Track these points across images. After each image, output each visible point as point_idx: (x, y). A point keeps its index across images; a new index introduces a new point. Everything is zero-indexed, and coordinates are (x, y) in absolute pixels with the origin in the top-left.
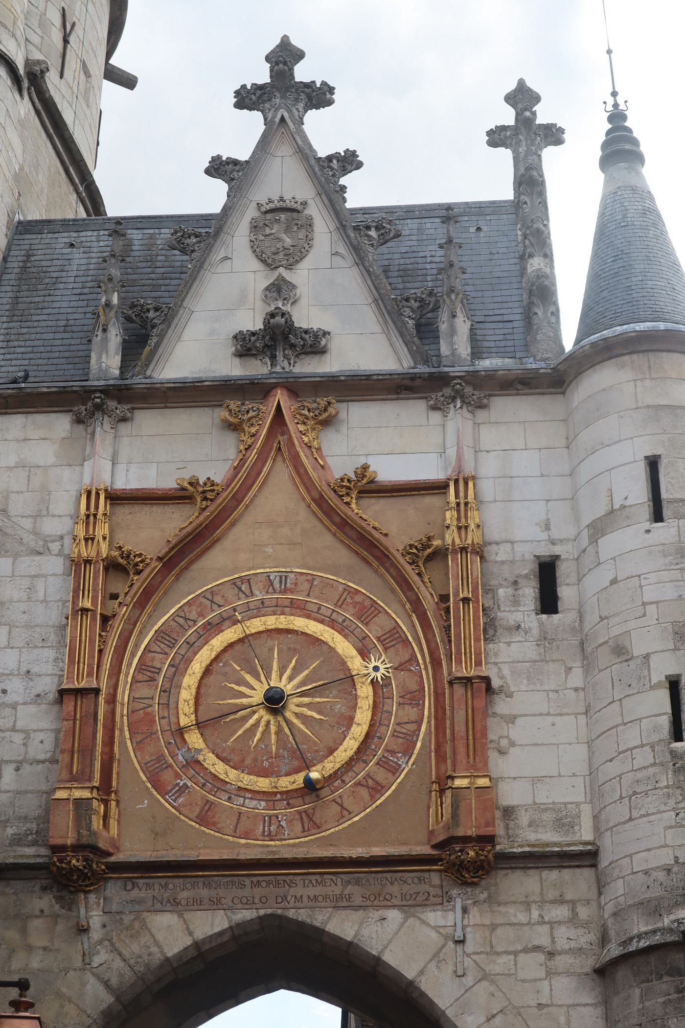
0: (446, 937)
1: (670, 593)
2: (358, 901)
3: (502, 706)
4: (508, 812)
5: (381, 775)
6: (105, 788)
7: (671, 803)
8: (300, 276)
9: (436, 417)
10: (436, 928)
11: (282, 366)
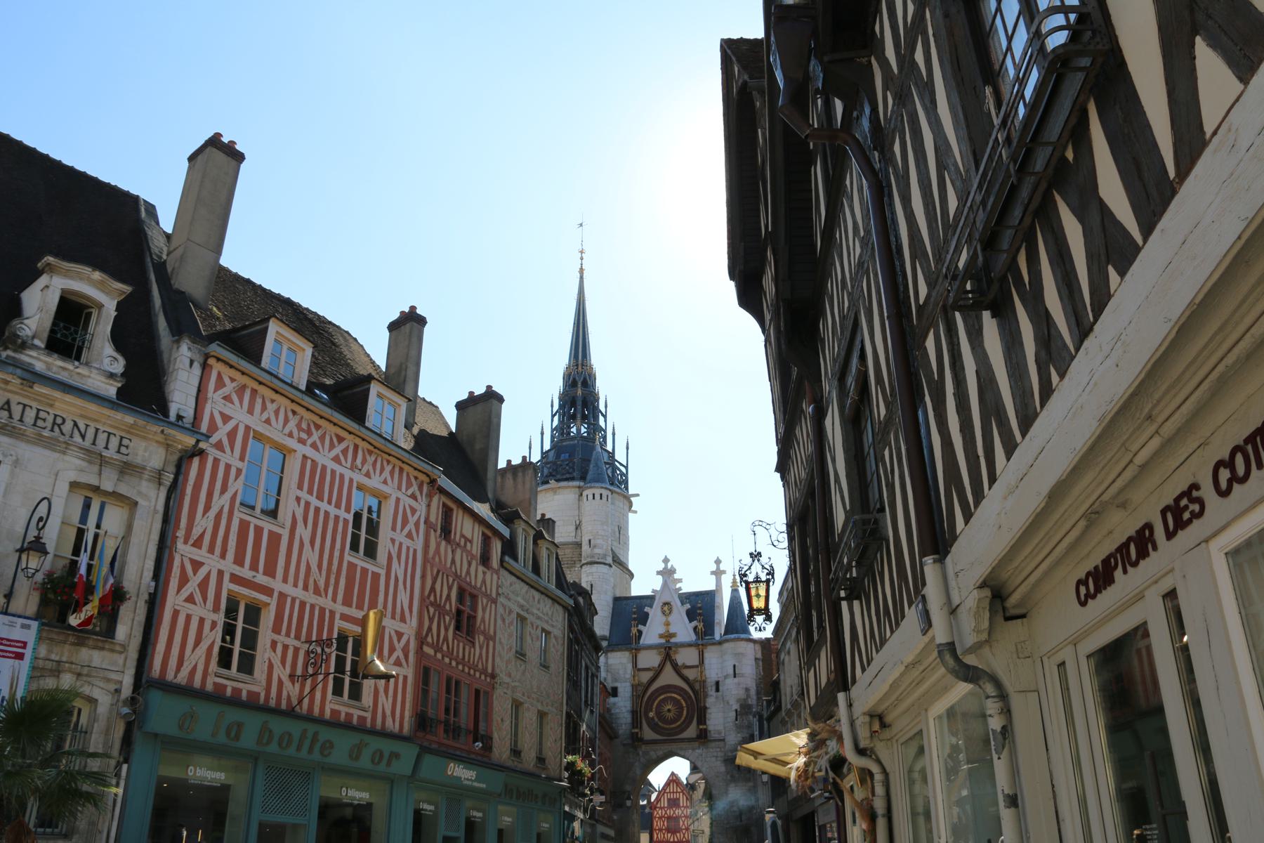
8: (670, 619)
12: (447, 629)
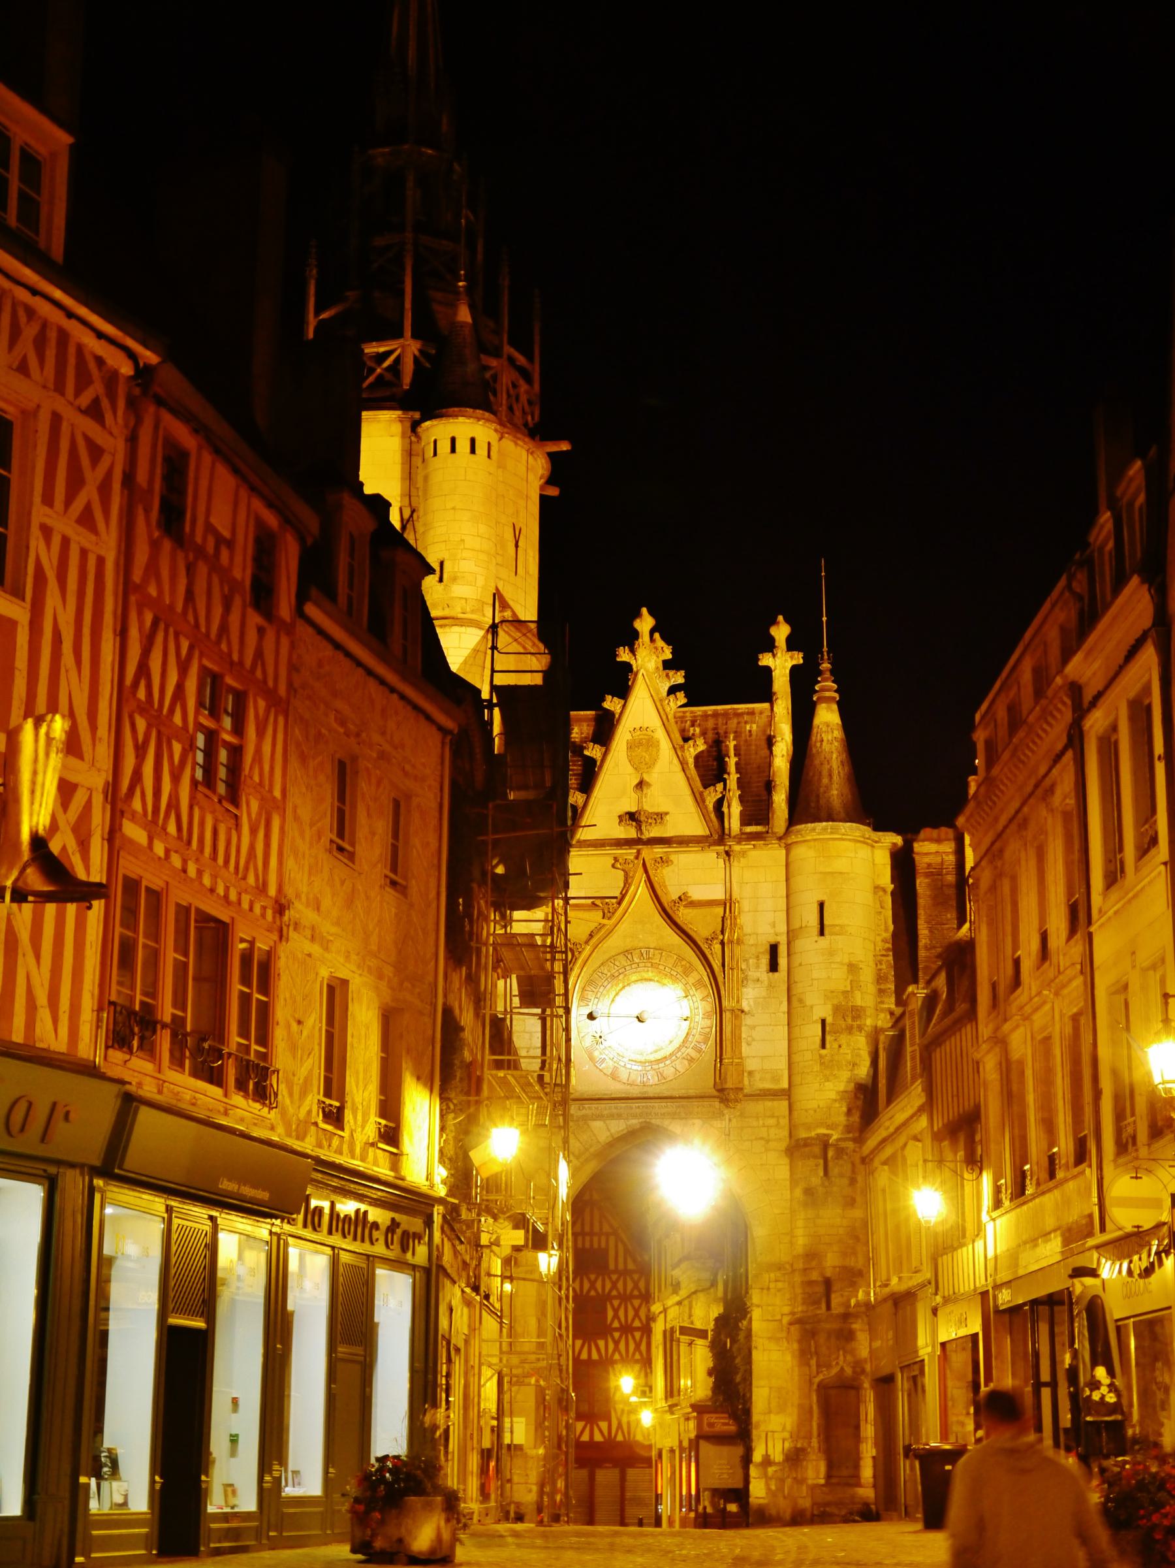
3: (747, 1021)
4: (750, 1073)
12: (176, 779)
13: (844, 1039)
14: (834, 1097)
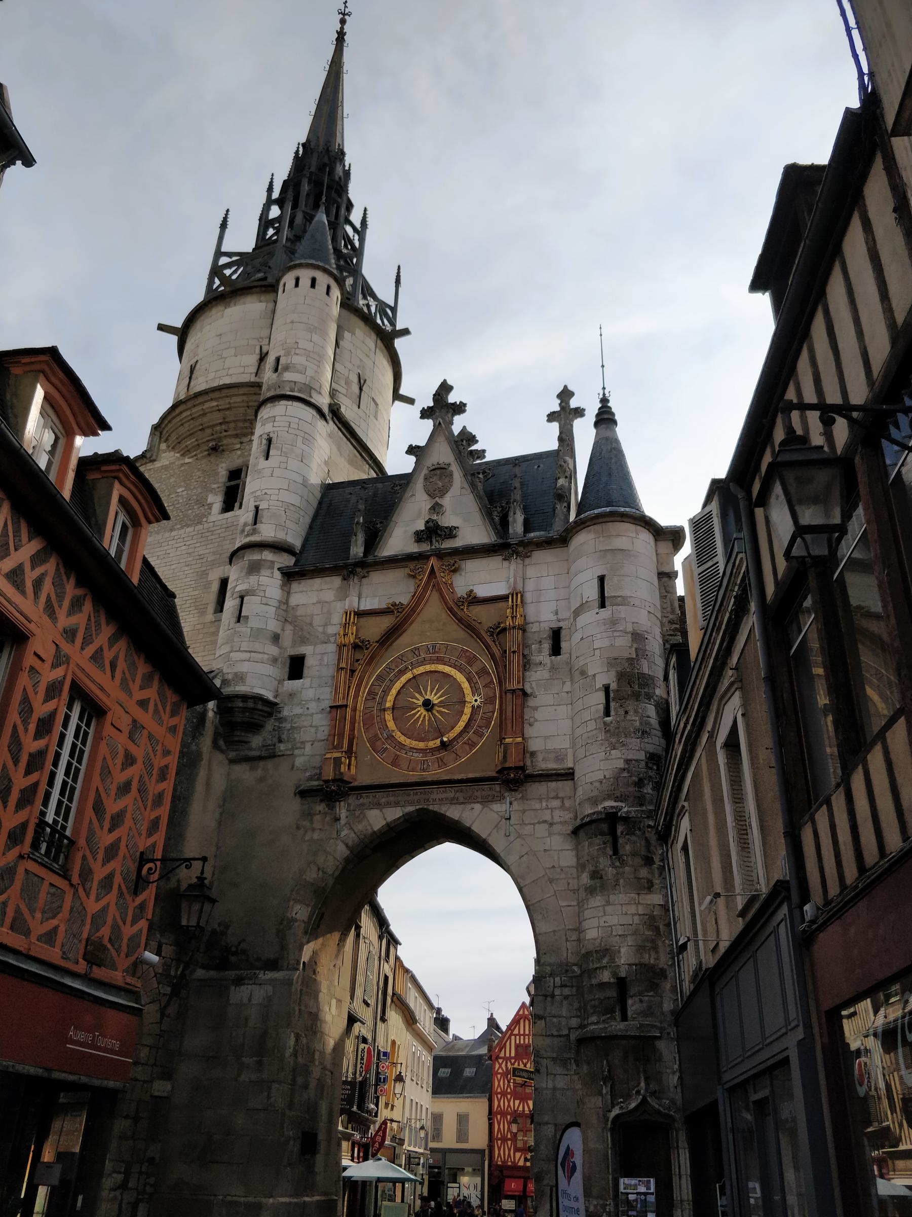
0: (502, 817)
1: (606, 643)
2: (461, 800)
3: (531, 702)
4: (533, 754)
5: (475, 738)
6: (349, 752)
7: (603, 748)
9: (506, 563)
10: (497, 812)
11: (436, 545)
13: (630, 705)
14: (622, 766)
